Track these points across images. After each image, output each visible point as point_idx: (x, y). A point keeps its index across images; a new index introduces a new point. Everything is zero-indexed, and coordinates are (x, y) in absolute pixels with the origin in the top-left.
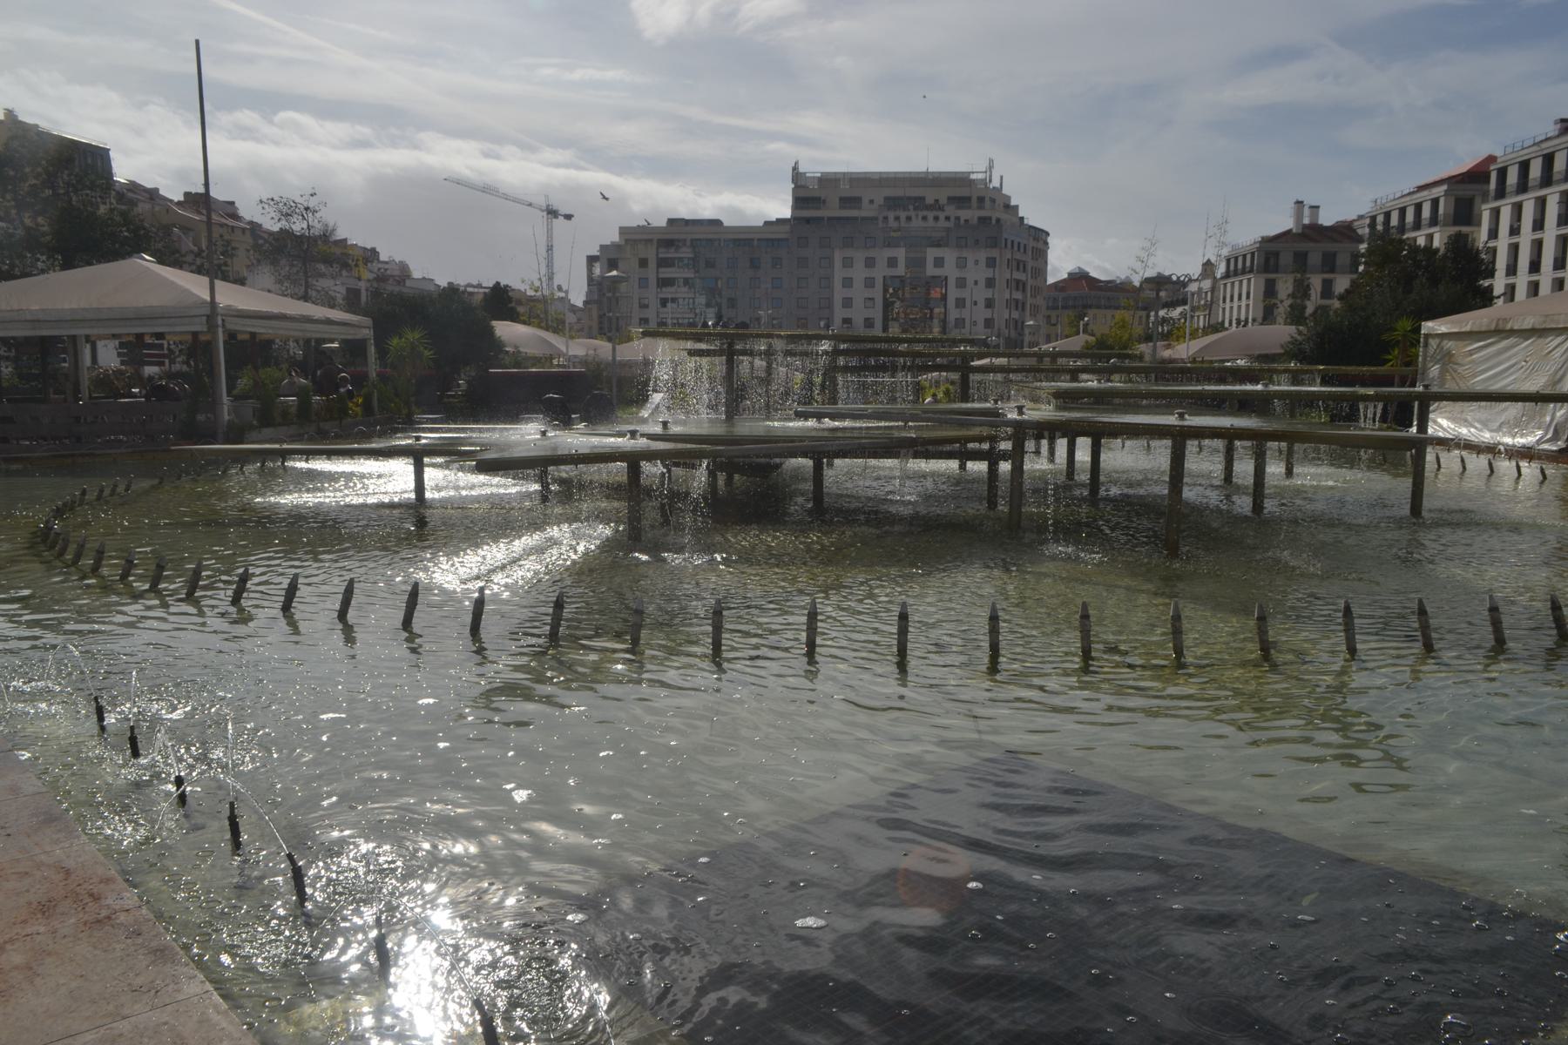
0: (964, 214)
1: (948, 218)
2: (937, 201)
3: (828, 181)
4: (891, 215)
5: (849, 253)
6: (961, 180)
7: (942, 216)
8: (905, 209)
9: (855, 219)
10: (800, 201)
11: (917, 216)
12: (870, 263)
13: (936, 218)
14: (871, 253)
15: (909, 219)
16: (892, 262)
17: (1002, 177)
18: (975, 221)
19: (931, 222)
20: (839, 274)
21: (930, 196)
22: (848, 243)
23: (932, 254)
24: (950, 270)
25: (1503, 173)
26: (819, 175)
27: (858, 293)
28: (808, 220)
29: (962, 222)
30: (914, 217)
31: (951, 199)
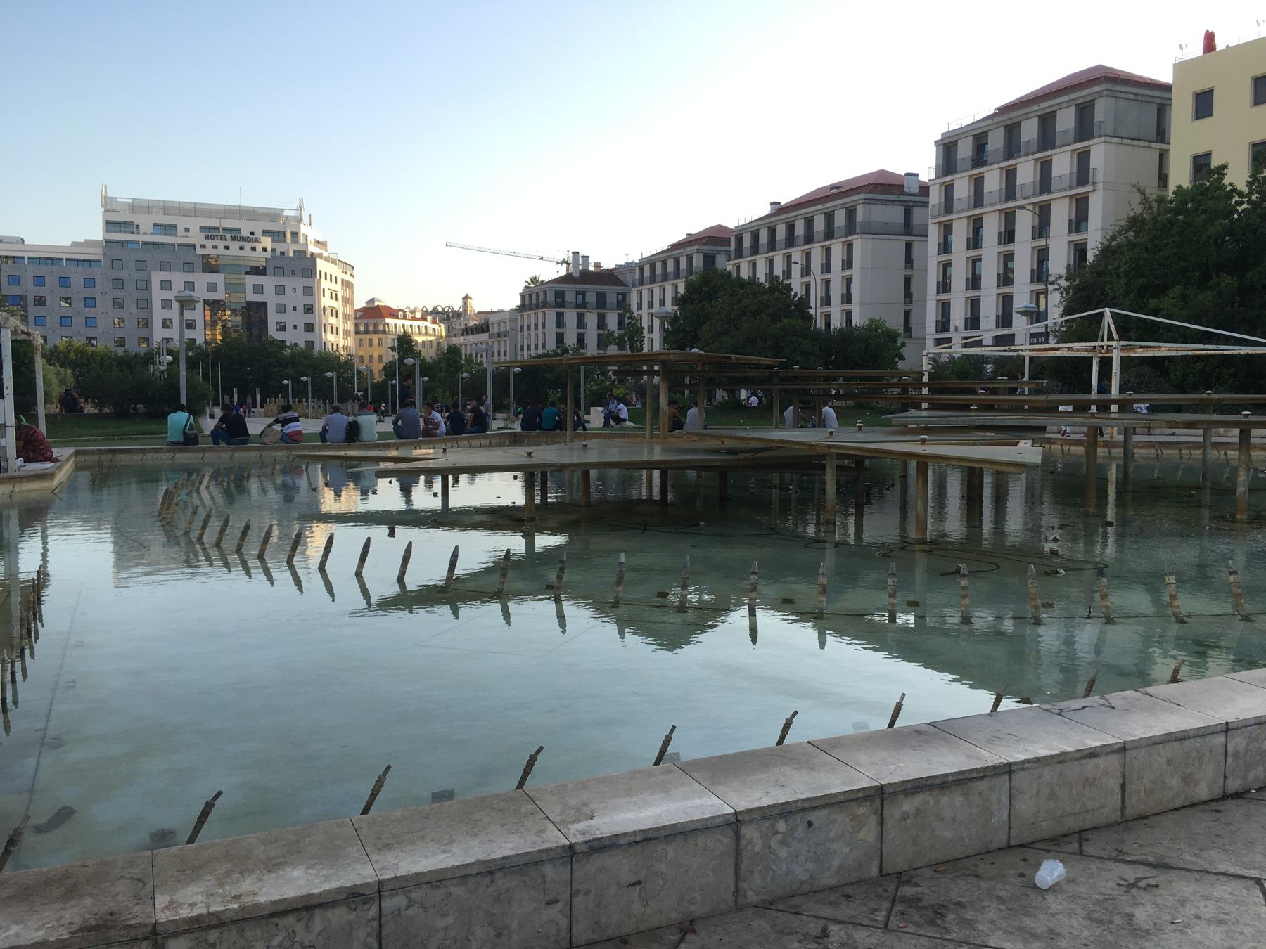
0: (280, 247)
2: (252, 234)
3: (138, 207)
4: (209, 243)
5: (165, 276)
6: (274, 215)
10: (110, 225)
14: (190, 277)
16: (212, 287)
20: (158, 296)
21: (246, 228)
22: (165, 266)
23: (251, 280)
24: (269, 296)
25: (739, 239)
26: (131, 201)
28: (123, 243)
29: (278, 254)
31: (266, 233)
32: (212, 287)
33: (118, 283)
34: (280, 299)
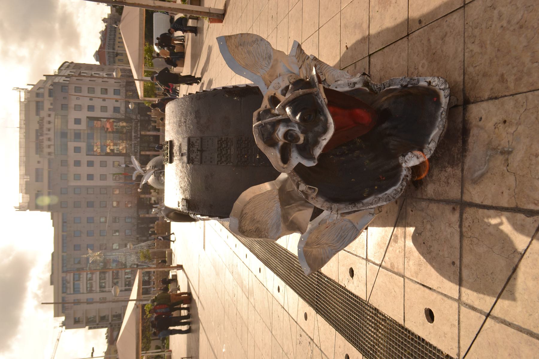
1: (49, 115)
4: (46, 150)
7: (47, 119)
8: (42, 141)
9: (49, 173)
11: (47, 134)
12: (77, 163)
13: (49, 122)
14: (71, 162)
15: (49, 139)
16: (77, 150)
17: (28, 85)
18: (51, 99)
19: (51, 126)
20: (84, 182)
27: (97, 171)
29: (52, 107)
30: (48, 136)
33: (77, 205)
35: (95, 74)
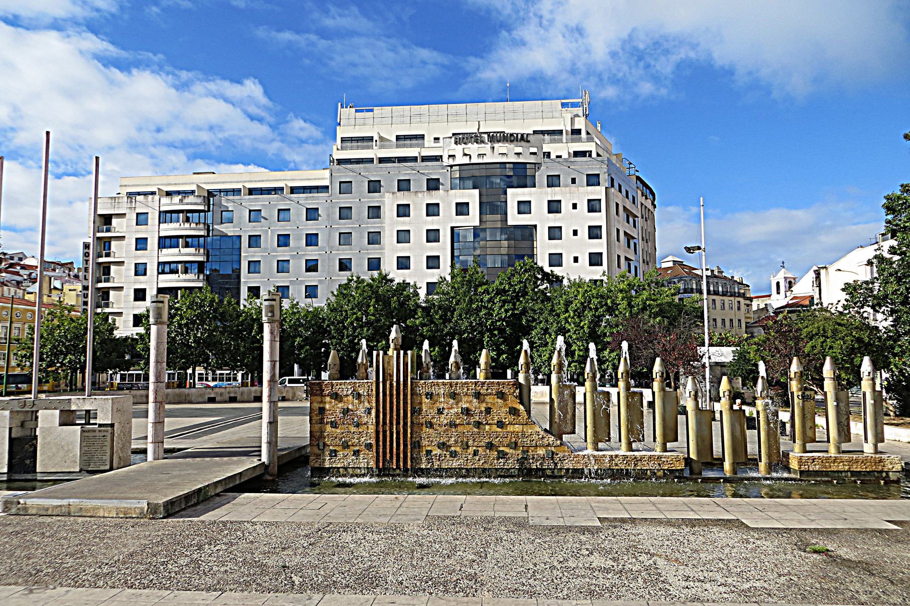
5: (403, 198)
12: (432, 210)
16: (462, 209)
22: (404, 185)
23: (514, 195)
24: (540, 218)
27: (418, 249)
32: (462, 209)
34: (554, 220)
35: (635, 244)
